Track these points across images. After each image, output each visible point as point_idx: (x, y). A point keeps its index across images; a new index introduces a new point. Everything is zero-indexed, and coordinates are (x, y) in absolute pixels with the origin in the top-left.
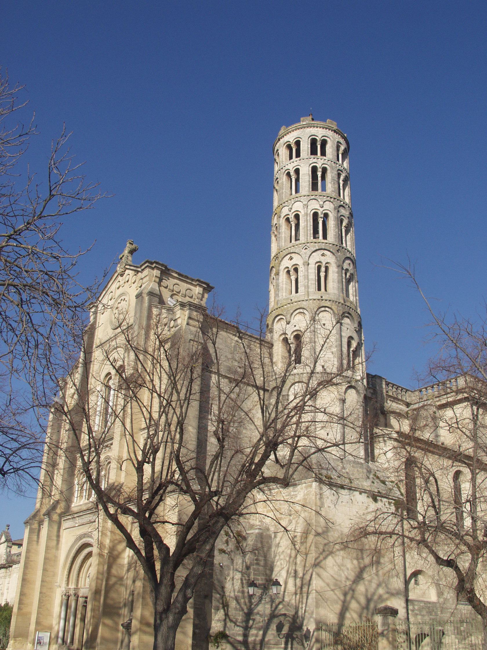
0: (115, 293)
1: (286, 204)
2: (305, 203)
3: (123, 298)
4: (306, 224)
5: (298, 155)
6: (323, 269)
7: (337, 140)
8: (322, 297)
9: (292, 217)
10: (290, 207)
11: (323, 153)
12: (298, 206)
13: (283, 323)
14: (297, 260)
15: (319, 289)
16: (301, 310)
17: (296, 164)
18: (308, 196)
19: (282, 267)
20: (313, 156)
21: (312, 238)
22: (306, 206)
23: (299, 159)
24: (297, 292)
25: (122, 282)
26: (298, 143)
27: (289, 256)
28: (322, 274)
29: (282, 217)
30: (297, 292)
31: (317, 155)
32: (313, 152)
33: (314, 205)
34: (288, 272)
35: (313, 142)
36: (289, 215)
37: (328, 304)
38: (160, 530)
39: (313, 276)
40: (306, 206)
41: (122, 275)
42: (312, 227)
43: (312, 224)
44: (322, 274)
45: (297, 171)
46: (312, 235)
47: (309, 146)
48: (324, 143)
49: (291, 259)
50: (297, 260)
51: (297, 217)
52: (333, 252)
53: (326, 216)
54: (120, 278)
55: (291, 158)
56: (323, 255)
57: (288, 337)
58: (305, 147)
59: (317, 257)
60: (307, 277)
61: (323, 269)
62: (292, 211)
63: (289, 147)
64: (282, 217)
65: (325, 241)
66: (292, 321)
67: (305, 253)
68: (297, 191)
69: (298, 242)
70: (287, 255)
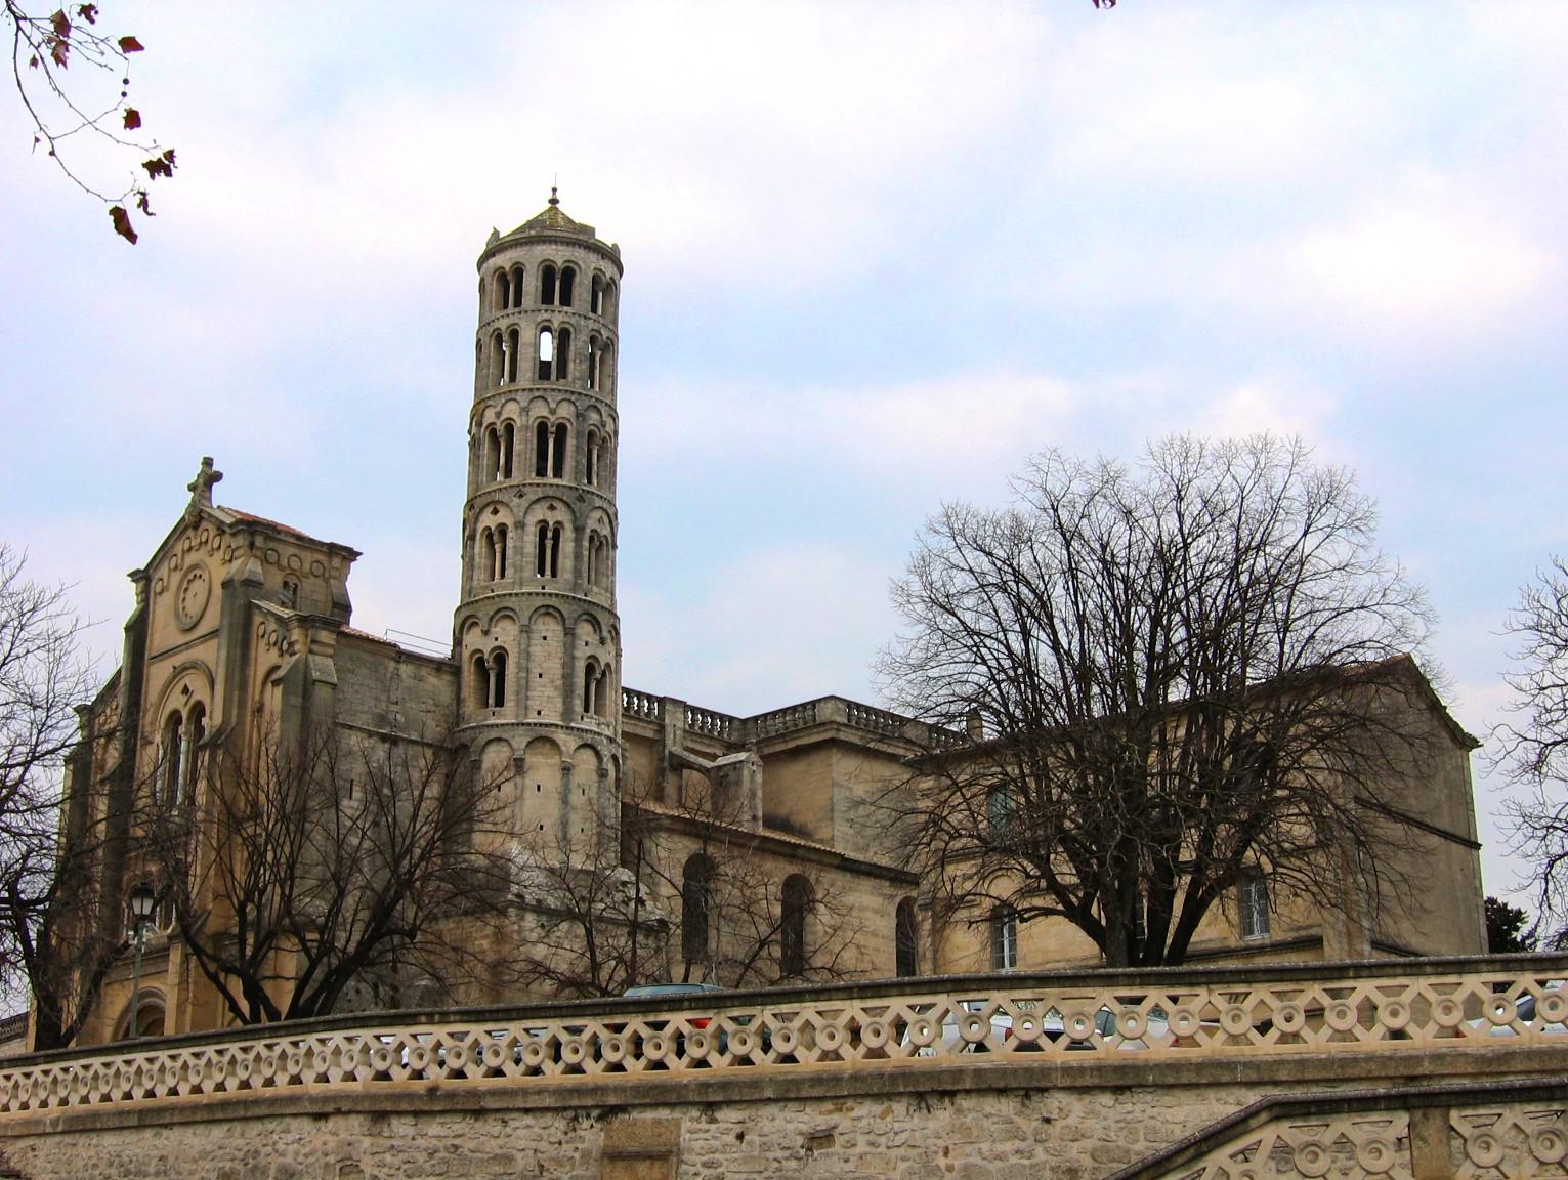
0: (183, 560)
1: (490, 402)
2: (524, 404)
3: (198, 572)
4: (524, 445)
5: (518, 303)
6: (550, 534)
7: (593, 266)
8: (543, 588)
9: (500, 429)
10: (498, 409)
11: (566, 300)
12: (511, 410)
13: (477, 631)
14: (504, 517)
15: (542, 571)
16: (508, 613)
17: (513, 320)
18: (531, 390)
19: (480, 527)
20: (544, 307)
21: (533, 474)
22: (526, 410)
23: (517, 310)
24: (503, 575)
25: (195, 543)
26: (519, 272)
27: (490, 509)
28: (549, 543)
29: (485, 425)
30: (503, 575)
31: (553, 303)
32: (547, 298)
33: (540, 410)
34: (490, 536)
35: (548, 272)
36: (494, 423)
37: (553, 602)
38: (268, 988)
39: (531, 548)
40: (526, 410)
41: (196, 527)
42: (534, 453)
43: (535, 446)
44: (549, 543)
45: (514, 335)
46: (534, 469)
47: (539, 284)
48: (568, 274)
49: (495, 512)
50: (504, 517)
51: (510, 429)
52: (569, 501)
53: (562, 430)
54: (190, 532)
55: (506, 306)
56: (552, 508)
57: (486, 657)
58: (532, 284)
59: (540, 513)
60: (519, 551)
61: (550, 534)
62: (502, 418)
63: (502, 277)
64: (485, 425)
65: (557, 481)
66: (493, 630)
67: (519, 505)
68: (513, 378)
69: (508, 483)
70: (488, 504)
